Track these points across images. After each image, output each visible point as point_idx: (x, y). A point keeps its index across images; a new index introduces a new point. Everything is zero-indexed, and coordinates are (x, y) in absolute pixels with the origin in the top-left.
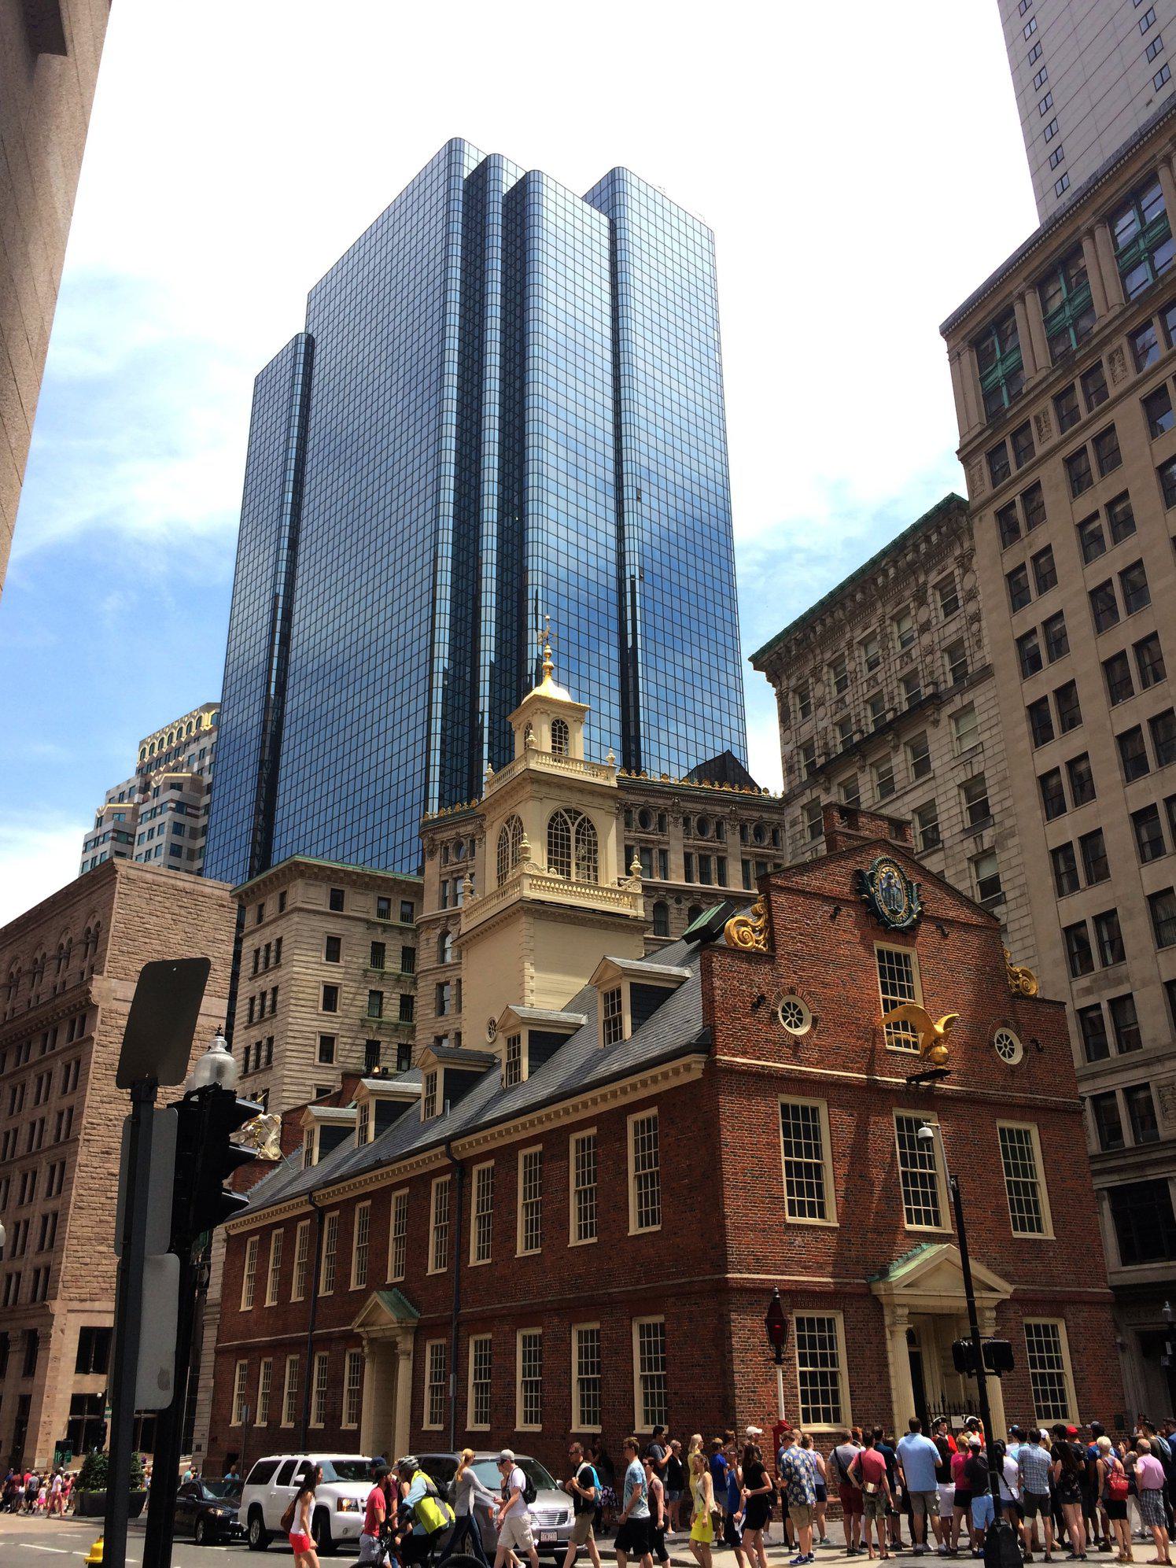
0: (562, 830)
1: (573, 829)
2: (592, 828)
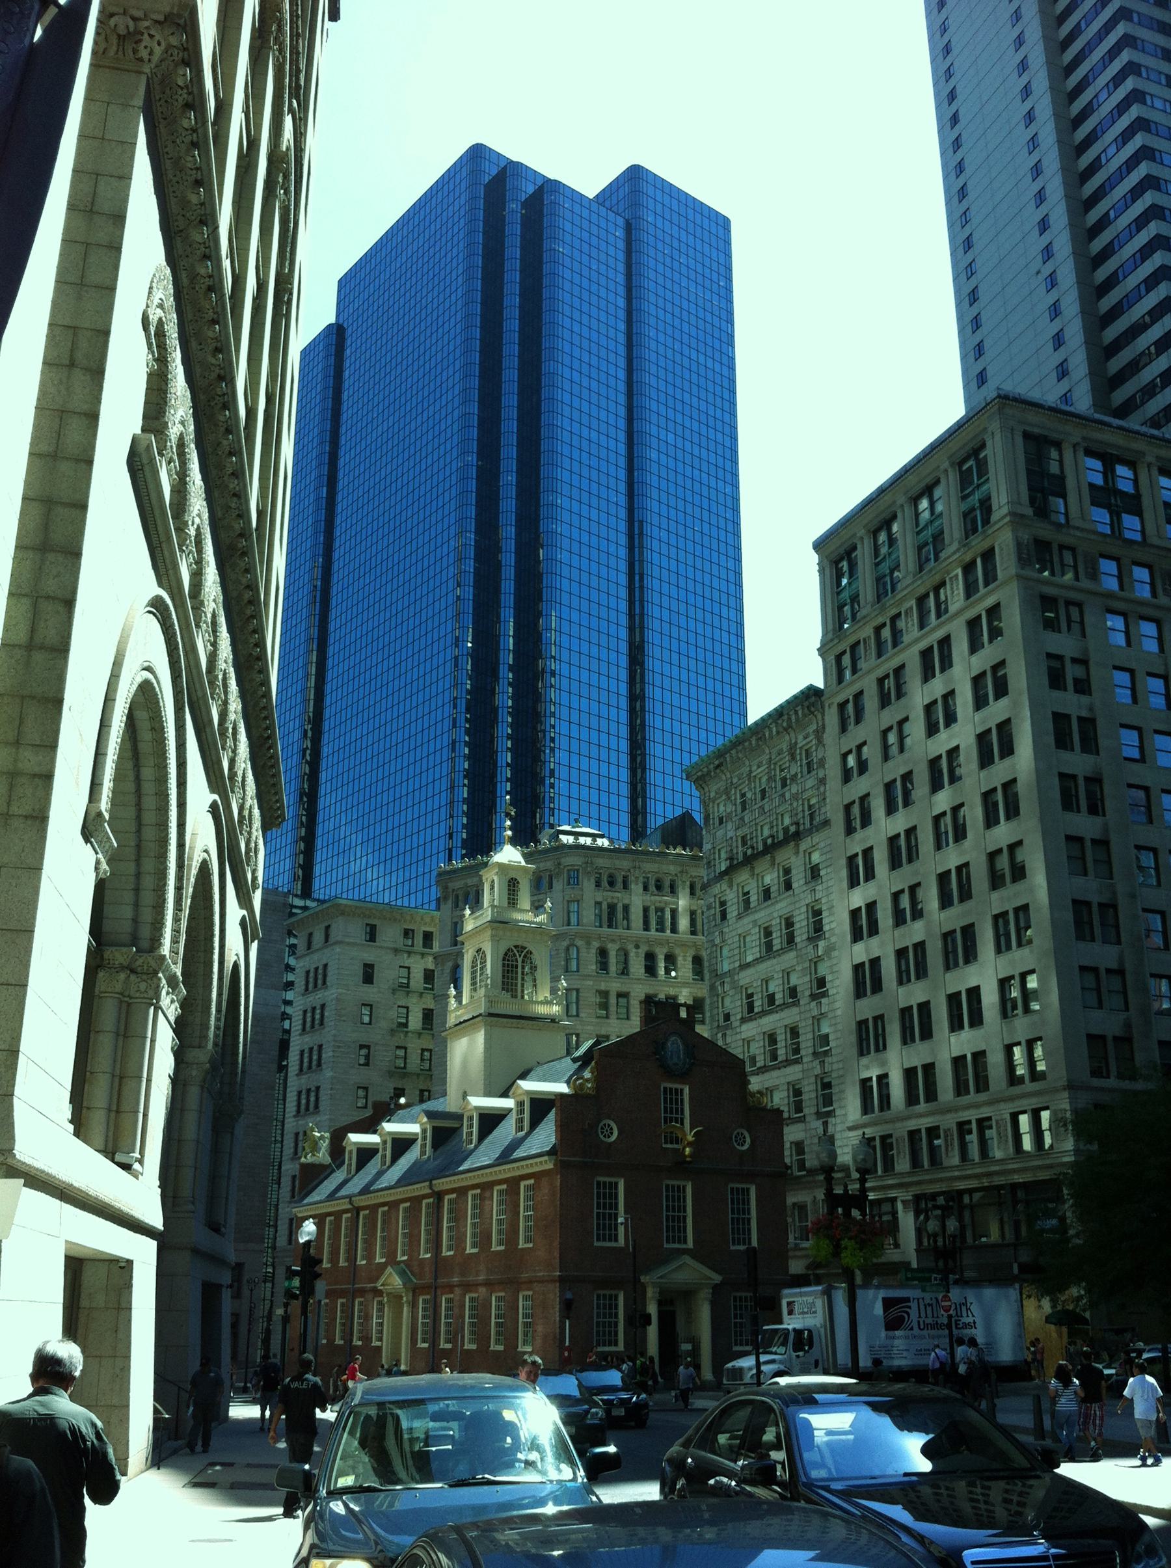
1: (520, 960)
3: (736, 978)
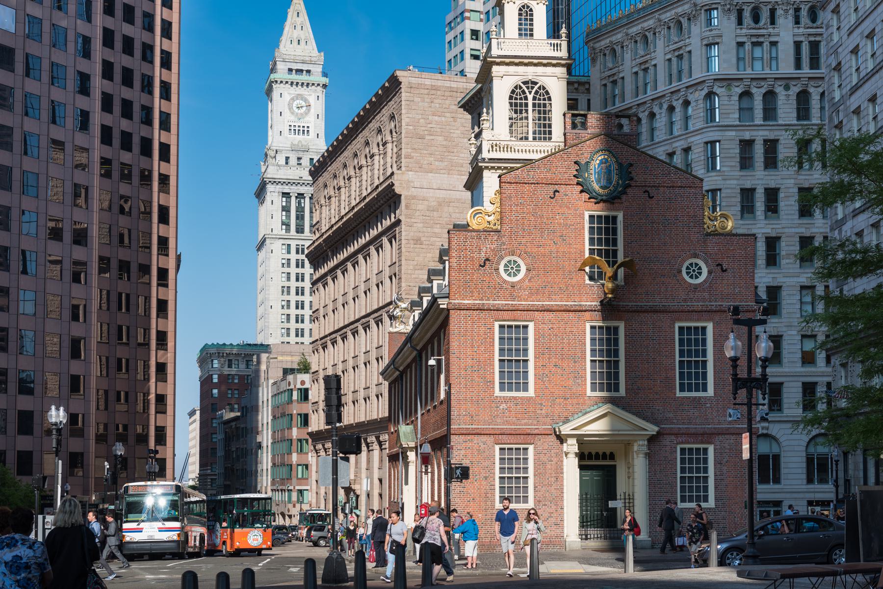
0: (521, 99)
1: (530, 97)
2: (547, 93)
3: (848, 104)
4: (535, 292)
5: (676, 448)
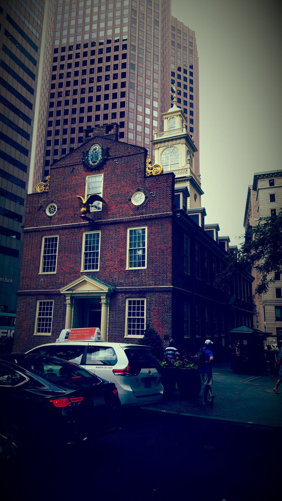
4: (60, 220)
5: (125, 301)
